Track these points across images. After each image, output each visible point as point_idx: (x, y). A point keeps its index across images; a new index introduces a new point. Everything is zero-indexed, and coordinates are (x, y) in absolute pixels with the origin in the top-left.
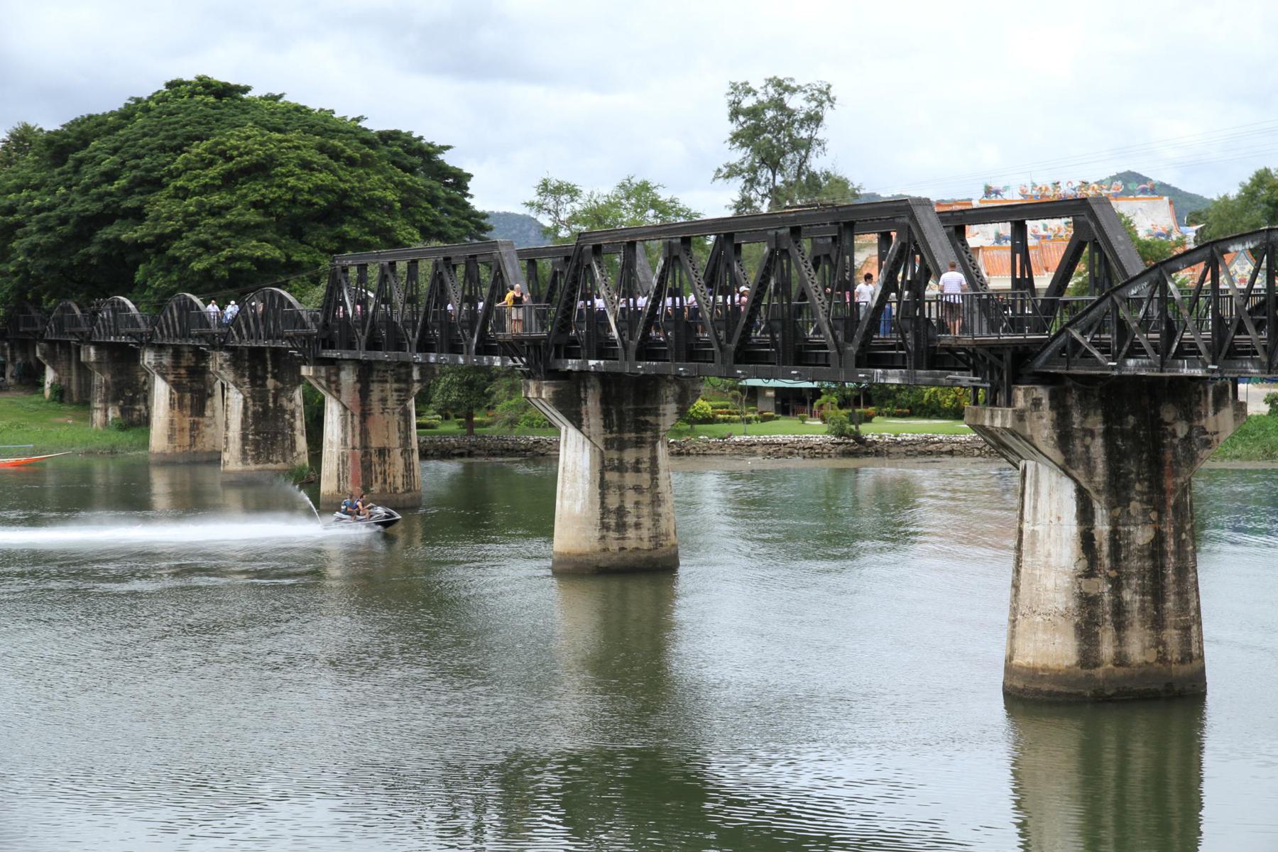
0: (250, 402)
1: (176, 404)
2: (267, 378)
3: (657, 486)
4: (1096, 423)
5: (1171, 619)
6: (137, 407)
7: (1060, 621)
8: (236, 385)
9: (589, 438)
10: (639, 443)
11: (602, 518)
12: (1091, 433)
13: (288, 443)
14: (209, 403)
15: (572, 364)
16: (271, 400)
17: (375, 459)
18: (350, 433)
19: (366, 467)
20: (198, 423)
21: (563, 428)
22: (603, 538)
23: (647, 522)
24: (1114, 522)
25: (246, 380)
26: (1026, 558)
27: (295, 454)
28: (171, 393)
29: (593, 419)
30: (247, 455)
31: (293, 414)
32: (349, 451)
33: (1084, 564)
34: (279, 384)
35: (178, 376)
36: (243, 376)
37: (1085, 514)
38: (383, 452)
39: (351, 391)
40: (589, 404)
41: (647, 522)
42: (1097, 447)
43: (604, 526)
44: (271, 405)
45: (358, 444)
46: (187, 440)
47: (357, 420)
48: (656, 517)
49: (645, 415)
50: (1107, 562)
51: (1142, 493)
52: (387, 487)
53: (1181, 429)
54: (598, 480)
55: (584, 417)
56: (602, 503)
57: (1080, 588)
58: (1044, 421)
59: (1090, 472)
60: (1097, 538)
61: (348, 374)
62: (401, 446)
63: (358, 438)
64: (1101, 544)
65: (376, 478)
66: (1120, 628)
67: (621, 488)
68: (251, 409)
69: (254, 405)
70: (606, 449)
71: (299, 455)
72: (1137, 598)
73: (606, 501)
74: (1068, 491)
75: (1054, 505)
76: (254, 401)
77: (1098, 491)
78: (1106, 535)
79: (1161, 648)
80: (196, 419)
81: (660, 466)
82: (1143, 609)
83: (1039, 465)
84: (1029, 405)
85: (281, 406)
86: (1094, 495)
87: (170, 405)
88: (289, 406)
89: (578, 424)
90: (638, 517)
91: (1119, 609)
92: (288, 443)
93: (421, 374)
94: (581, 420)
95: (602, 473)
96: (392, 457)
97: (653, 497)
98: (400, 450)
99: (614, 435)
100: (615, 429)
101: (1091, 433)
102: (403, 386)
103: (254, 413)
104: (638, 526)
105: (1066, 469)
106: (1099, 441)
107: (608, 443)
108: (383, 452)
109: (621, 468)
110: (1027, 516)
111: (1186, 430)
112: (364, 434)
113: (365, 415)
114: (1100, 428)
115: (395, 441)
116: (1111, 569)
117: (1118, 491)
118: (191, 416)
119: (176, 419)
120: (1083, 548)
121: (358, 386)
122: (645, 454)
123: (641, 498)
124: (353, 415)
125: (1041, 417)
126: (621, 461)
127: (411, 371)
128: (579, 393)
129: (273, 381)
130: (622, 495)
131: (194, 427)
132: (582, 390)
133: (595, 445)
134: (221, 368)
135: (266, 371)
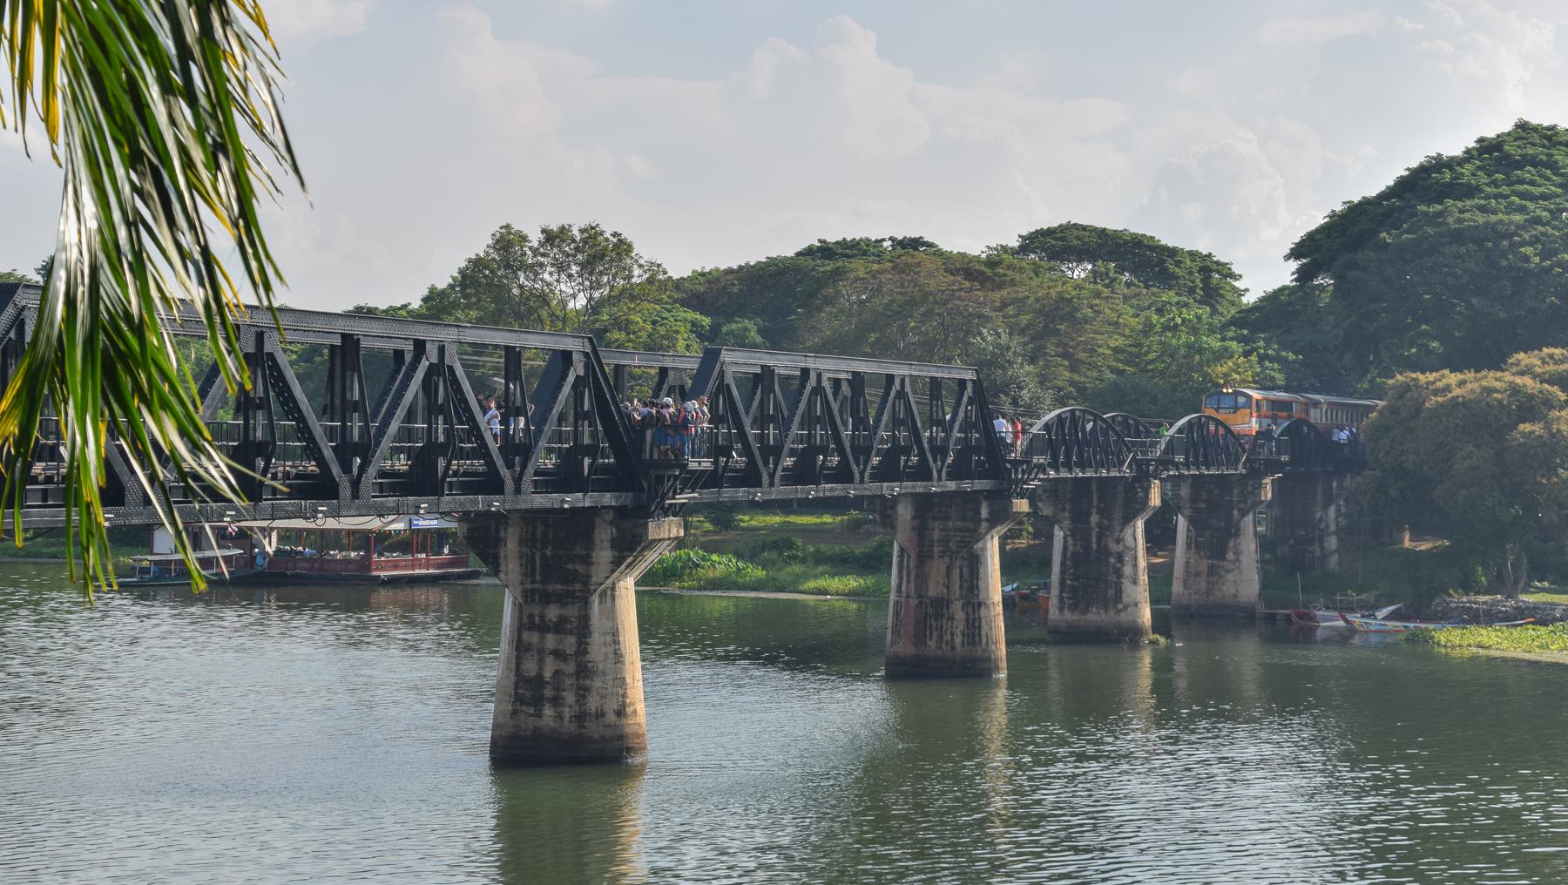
0: (1070, 541)
2: (1091, 514)
3: (586, 652)
6: (1310, 548)
10: (562, 599)
11: (515, 690)
13: (1111, 592)
14: (1231, 544)
20: (1218, 567)
22: (515, 713)
23: (570, 697)
25: (1067, 514)
27: (1120, 606)
30: (1065, 603)
31: (1120, 557)
36: (1064, 510)
38: (941, 604)
39: (908, 528)
40: (509, 546)
41: (570, 697)
43: (518, 699)
44: (1094, 546)
45: (912, 593)
46: (1203, 586)
48: (583, 692)
49: (574, 564)
52: (944, 645)
54: (515, 640)
55: (502, 560)
56: (518, 669)
61: (906, 509)
62: (962, 597)
63: (912, 585)
65: (931, 634)
68: (1071, 548)
69: (1075, 545)
70: (526, 602)
71: (1126, 607)
73: (522, 666)
76: (1074, 540)
80: (1215, 562)
81: (592, 629)
85: (1106, 547)
92: (1111, 592)
93: (991, 513)
96: (951, 610)
97: (578, 665)
98: (961, 602)
99: (536, 586)
100: (538, 578)
102: (970, 525)
103: (1075, 554)
104: (556, 701)
107: (528, 596)
108: (941, 604)
109: (543, 628)
113: (924, 557)
118: (1209, 558)
119: (1192, 561)
121: (916, 522)
122: (572, 611)
123: (563, 667)
124: (909, 556)
126: (542, 617)
127: (980, 508)
128: (497, 531)
130: (541, 661)
131: (1212, 571)
132: (502, 528)
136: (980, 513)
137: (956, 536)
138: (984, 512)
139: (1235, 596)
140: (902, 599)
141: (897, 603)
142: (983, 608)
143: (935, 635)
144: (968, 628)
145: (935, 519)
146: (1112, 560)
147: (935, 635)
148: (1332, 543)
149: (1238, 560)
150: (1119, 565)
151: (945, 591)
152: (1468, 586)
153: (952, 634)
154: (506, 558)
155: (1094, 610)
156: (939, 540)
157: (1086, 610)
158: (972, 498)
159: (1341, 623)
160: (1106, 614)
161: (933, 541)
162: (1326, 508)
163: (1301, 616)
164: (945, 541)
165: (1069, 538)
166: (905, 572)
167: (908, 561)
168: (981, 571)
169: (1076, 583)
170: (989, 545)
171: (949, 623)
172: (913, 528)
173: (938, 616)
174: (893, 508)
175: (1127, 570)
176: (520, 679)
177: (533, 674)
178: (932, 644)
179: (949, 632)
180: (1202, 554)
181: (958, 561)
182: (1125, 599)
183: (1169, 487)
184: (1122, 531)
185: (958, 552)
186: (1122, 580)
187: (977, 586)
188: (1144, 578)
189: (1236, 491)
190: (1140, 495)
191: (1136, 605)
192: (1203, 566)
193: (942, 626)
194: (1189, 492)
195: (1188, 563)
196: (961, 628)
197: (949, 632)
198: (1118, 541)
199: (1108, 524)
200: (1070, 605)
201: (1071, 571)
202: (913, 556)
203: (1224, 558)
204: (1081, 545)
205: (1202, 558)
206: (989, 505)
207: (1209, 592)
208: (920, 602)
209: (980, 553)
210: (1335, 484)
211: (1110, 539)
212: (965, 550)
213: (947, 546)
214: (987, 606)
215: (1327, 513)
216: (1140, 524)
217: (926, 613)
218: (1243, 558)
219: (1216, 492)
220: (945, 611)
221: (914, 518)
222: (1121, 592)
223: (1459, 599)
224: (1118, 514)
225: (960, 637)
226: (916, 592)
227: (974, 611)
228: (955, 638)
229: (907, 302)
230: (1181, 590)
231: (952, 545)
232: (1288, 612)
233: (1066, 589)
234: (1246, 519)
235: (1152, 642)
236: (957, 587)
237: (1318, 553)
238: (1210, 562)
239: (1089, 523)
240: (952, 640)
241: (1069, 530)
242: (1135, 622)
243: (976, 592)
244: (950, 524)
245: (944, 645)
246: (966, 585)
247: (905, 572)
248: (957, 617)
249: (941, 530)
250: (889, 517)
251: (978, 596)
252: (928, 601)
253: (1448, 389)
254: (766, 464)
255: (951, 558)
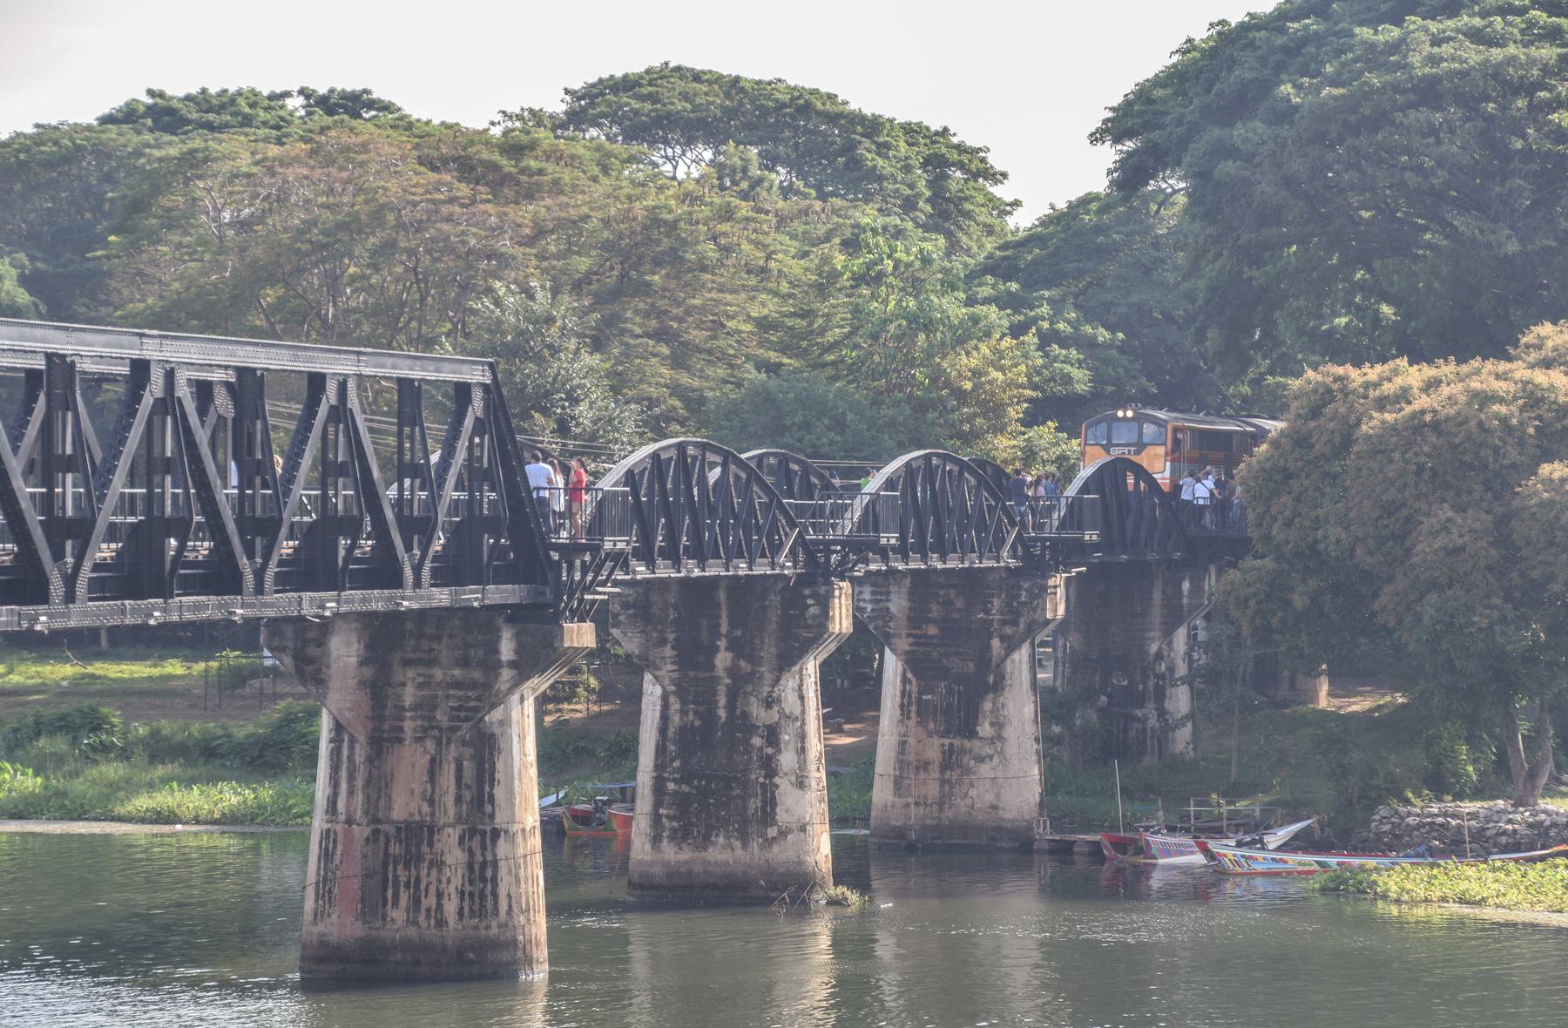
0: (675, 705)
1: (913, 707)
2: (717, 649)
6: (1138, 713)
13: (754, 804)
16: (722, 701)
18: (344, 786)
25: (668, 651)
27: (772, 832)
31: (772, 735)
32: (339, 828)
34: (743, 663)
35: (919, 640)
36: (663, 642)
38: (418, 834)
39: (352, 683)
44: (722, 713)
45: (359, 813)
46: (933, 790)
52: (422, 918)
61: (348, 644)
62: (459, 819)
63: (359, 797)
65: (396, 895)
68: (676, 719)
69: (684, 712)
71: (783, 834)
76: (684, 702)
80: (957, 742)
87: (902, 706)
92: (754, 804)
96: (438, 846)
98: (459, 830)
102: (477, 675)
103: (683, 730)
108: (418, 834)
113: (383, 741)
118: (944, 734)
119: (911, 740)
121: (368, 672)
124: (352, 741)
127: (499, 638)
129: (730, 655)
131: (950, 760)
135: (716, 634)
136: (497, 651)
137: (448, 697)
138: (507, 649)
139: (994, 807)
140: (339, 828)
141: (327, 835)
142: (501, 842)
143: (404, 898)
144: (471, 883)
145: (407, 663)
146: (757, 741)
147: (404, 898)
148: (1180, 700)
149: (1000, 737)
150: (770, 751)
151: (426, 808)
152: (1440, 783)
153: (440, 895)
155: (721, 840)
156: (416, 707)
157: (705, 841)
158: (482, 622)
159: (1198, 859)
160: (744, 846)
161: (403, 709)
162: (1168, 633)
163: (1121, 846)
164: (426, 708)
165: (672, 699)
166: (344, 774)
167: (352, 748)
168: (499, 766)
169: (685, 788)
170: (515, 714)
171: (434, 873)
172: (361, 683)
173: (412, 859)
174: (321, 643)
175: (787, 760)
178: (398, 915)
179: (432, 890)
180: (931, 725)
181: (452, 747)
182: (782, 817)
183: (867, 596)
184: (777, 681)
185: (453, 730)
186: (777, 780)
187: (491, 796)
188: (818, 776)
189: (996, 602)
190: (813, 610)
191: (803, 829)
192: (933, 749)
193: (418, 880)
194: (904, 603)
195: (903, 744)
196: (457, 881)
197: (432, 890)
198: (769, 703)
199: (749, 669)
200: (674, 831)
201: (677, 764)
202: (361, 738)
203: (972, 734)
204: (696, 713)
205: (930, 735)
206: (517, 636)
207: (941, 804)
208: (376, 832)
209: (497, 730)
210: (1186, 586)
211: (753, 699)
212: (466, 726)
213: (431, 718)
214: (511, 838)
215: (1170, 644)
216: (811, 668)
217: (387, 855)
218: (1010, 732)
219: (959, 604)
220: (425, 849)
221: (363, 663)
222: (774, 804)
223: (1423, 808)
224: (769, 651)
225: (455, 900)
226: (366, 813)
227: (484, 848)
228: (445, 901)
229: (342, 226)
230: (891, 798)
231: (442, 717)
232: (1098, 838)
233: (667, 799)
234: (1016, 656)
235: (833, 902)
236: (450, 799)
237: (1153, 722)
238: (947, 741)
239: (712, 667)
240: (440, 906)
241: (673, 682)
242: (800, 863)
243: (488, 808)
244: (438, 674)
245: (422, 918)
246: (467, 795)
247: (344, 774)
248: (449, 860)
249: (420, 686)
250: (311, 661)
251: (492, 816)
252: (391, 830)
253: (1404, 396)
254: (58, 556)
255: (439, 744)
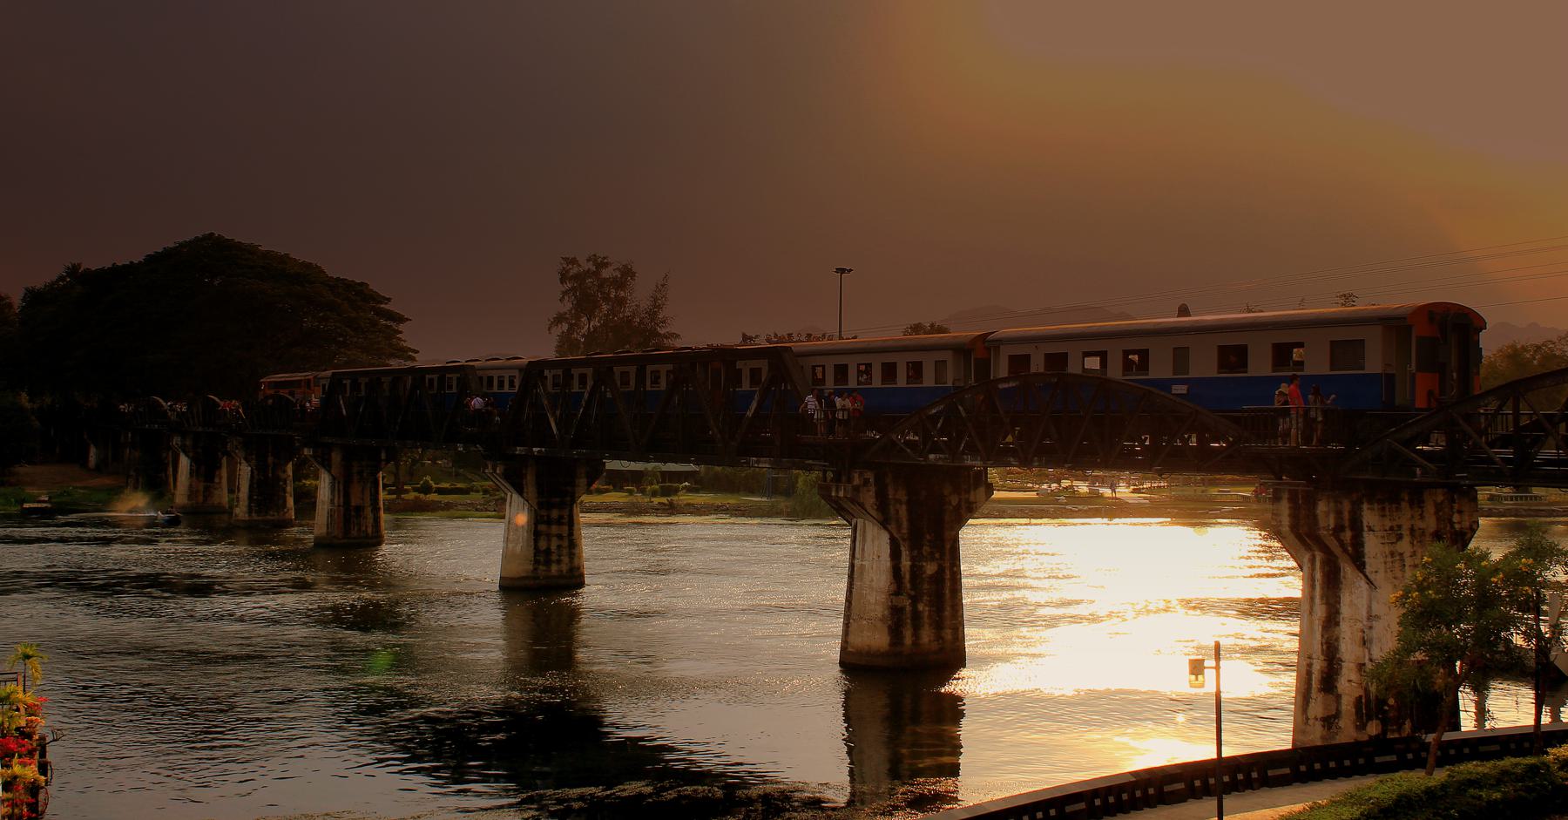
0: (256, 472)
4: (902, 495)
5: (948, 623)
7: (879, 624)
8: (246, 459)
9: (527, 501)
11: (535, 556)
12: (900, 502)
14: (217, 473)
15: (519, 450)
17: (353, 513)
18: (337, 496)
19: (347, 521)
21: (509, 494)
22: (535, 569)
23: (565, 559)
24: (913, 559)
25: (254, 457)
26: (857, 583)
27: (286, 510)
28: (191, 465)
29: (531, 489)
33: (894, 587)
37: (895, 555)
40: (529, 477)
41: (565, 559)
42: (903, 512)
43: (537, 562)
47: (341, 488)
48: (572, 556)
50: (908, 585)
51: (929, 541)
53: (954, 500)
55: (525, 486)
57: (892, 602)
58: (871, 493)
59: (899, 528)
60: (903, 569)
62: (372, 504)
64: (905, 574)
66: (916, 629)
67: (549, 536)
68: (256, 477)
72: (927, 609)
74: (884, 539)
75: (876, 548)
77: (904, 540)
78: (908, 568)
79: (940, 641)
82: (930, 617)
83: (866, 522)
84: (862, 482)
86: (901, 542)
88: (283, 476)
89: (520, 492)
90: (560, 556)
91: (916, 616)
94: (523, 488)
95: (536, 525)
101: (900, 502)
104: (559, 562)
105: (884, 524)
106: (904, 507)
107: (540, 505)
108: (359, 510)
109: (549, 523)
110: (857, 555)
111: (957, 500)
112: (347, 495)
114: (904, 498)
115: (368, 502)
116: (911, 590)
117: (915, 541)
120: (894, 576)
124: (339, 483)
125: (869, 491)
126: (548, 516)
130: (549, 540)
131: (207, 489)
133: (532, 506)
134: (237, 448)
138: (383, 456)
154: (526, 484)
165: (255, 471)
176: (537, 551)
177: (544, 548)
178: (354, 533)
192: (201, 486)
203: (213, 482)
230: (186, 502)
247: (336, 493)
